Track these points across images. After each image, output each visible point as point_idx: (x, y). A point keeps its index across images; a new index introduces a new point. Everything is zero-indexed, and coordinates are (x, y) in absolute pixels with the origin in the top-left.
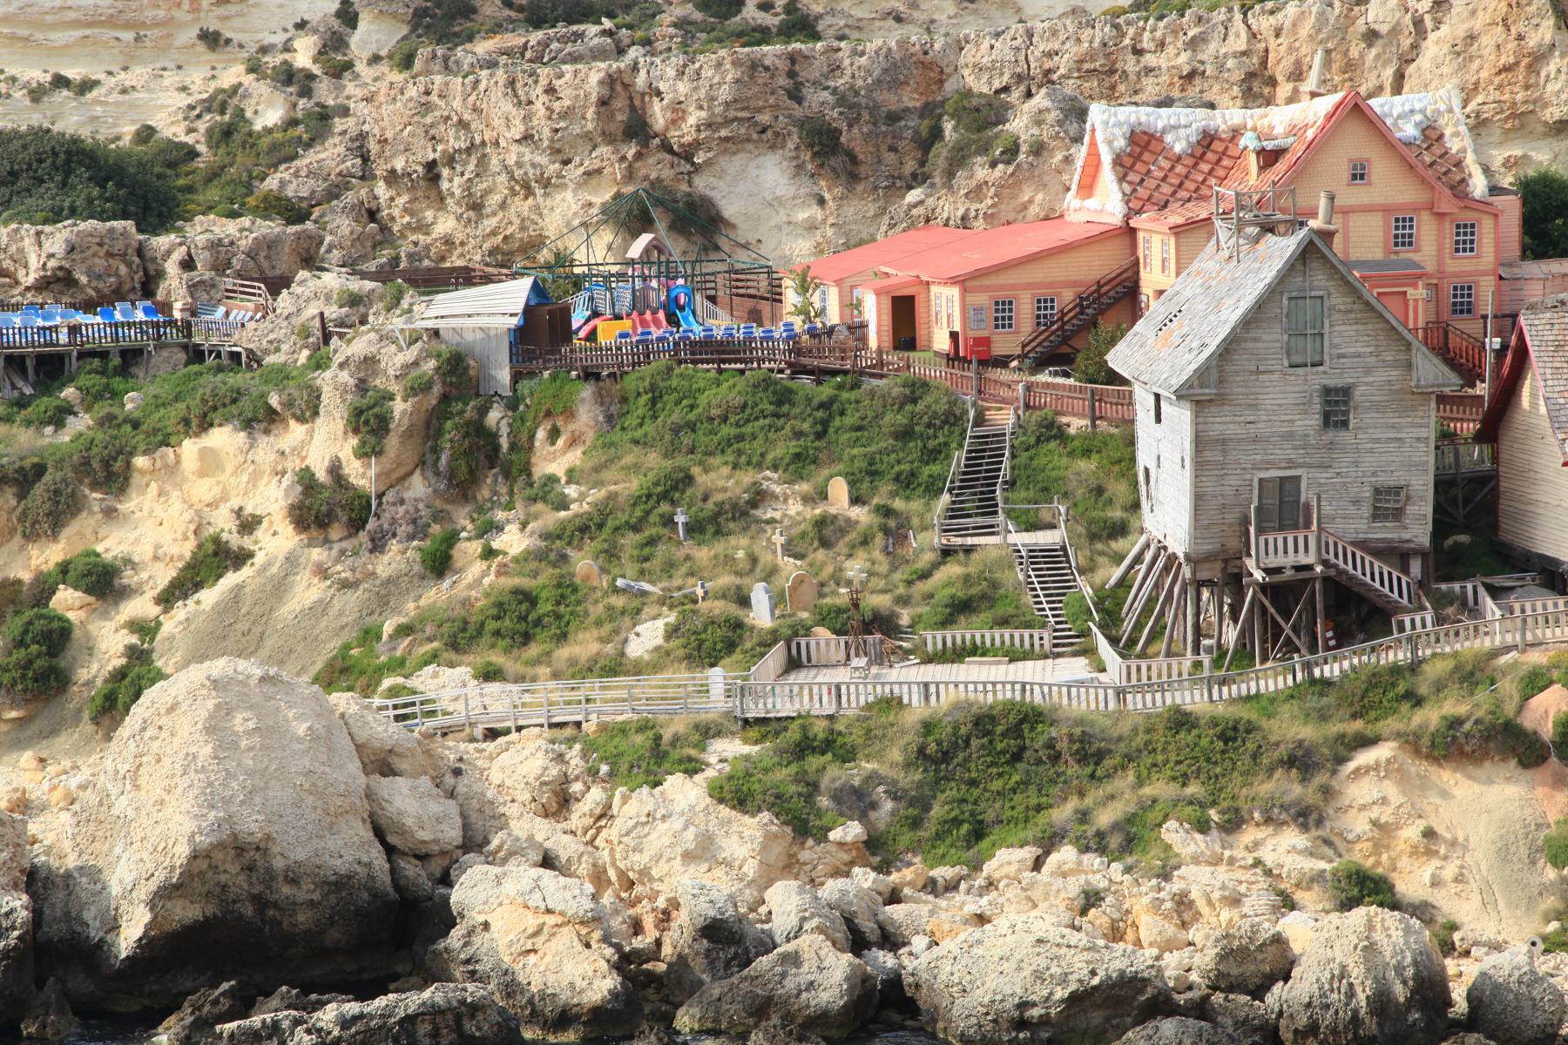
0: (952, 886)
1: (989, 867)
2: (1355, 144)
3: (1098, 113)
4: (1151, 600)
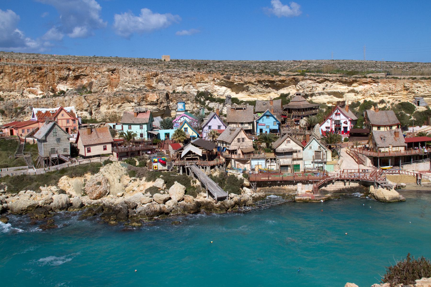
0: (14, 196)
1: (20, 193)
3: (34, 109)
4: (40, 162)
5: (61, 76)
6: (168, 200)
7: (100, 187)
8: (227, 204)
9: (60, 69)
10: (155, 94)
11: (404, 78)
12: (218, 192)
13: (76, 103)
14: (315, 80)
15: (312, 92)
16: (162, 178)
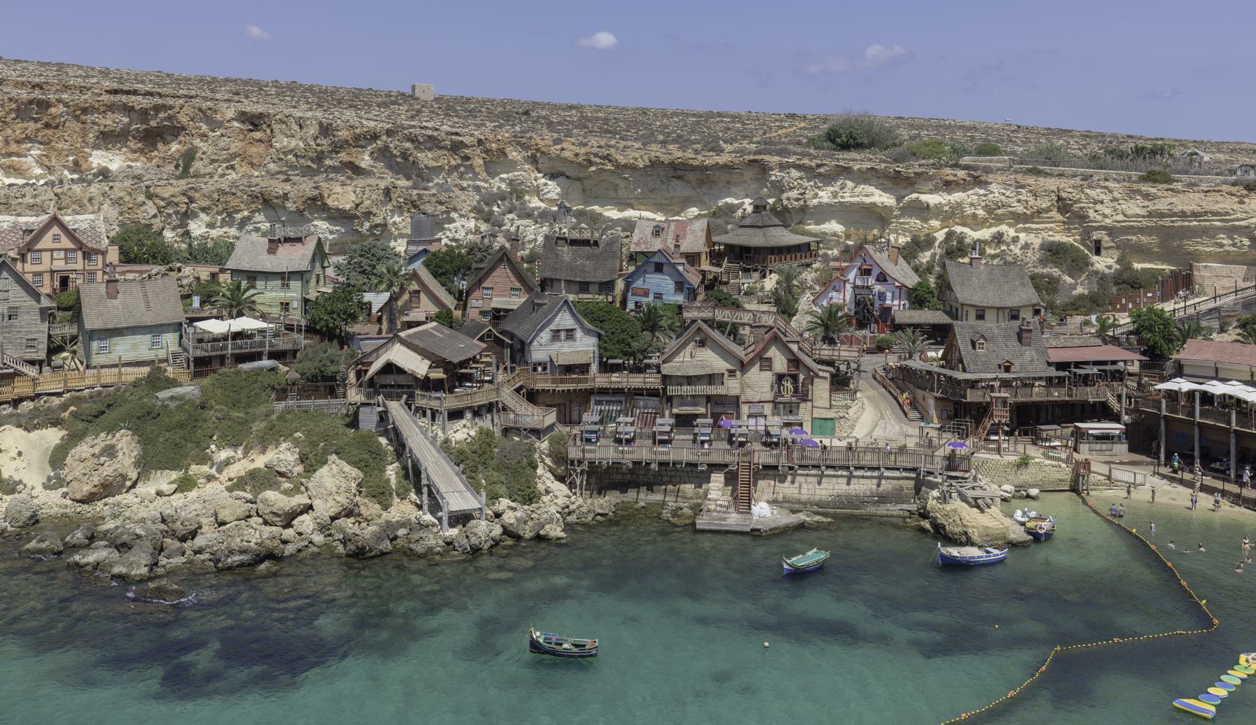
2: (55, 230)
5: (105, 126)
6: (301, 513)
7: (106, 464)
8: (476, 535)
9: (102, 109)
10: (350, 189)
11: (1061, 175)
12: (458, 498)
13: (120, 205)
14: (811, 168)
15: (802, 202)
16: (296, 442)
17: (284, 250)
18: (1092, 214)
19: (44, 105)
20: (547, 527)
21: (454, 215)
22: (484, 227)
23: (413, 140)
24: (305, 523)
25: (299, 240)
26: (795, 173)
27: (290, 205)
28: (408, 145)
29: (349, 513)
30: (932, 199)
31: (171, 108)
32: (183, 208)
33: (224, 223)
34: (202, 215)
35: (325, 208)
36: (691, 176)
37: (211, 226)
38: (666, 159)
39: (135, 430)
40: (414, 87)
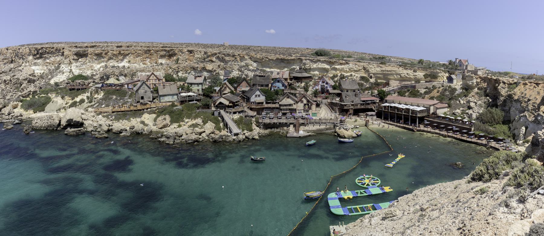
2: (153, 75)
11: (364, 62)
12: (235, 130)
16: (202, 118)
17: (198, 78)
18: (370, 70)
19: (149, 51)
20: (255, 136)
21: (233, 70)
22: (240, 73)
23: (224, 54)
24: (204, 135)
25: (201, 76)
26: (308, 61)
27: (199, 69)
28: (223, 56)
29: (213, 133)
30: (337, 67)
31: (174, 50)
32: (177, 70)
33: (185, 73)
34: (181, 72)
35: (206, 69)
36: (285, 62)
37: (183, 74)
38: (280, 58)
39: (169, 115)
40: (224, 43)
